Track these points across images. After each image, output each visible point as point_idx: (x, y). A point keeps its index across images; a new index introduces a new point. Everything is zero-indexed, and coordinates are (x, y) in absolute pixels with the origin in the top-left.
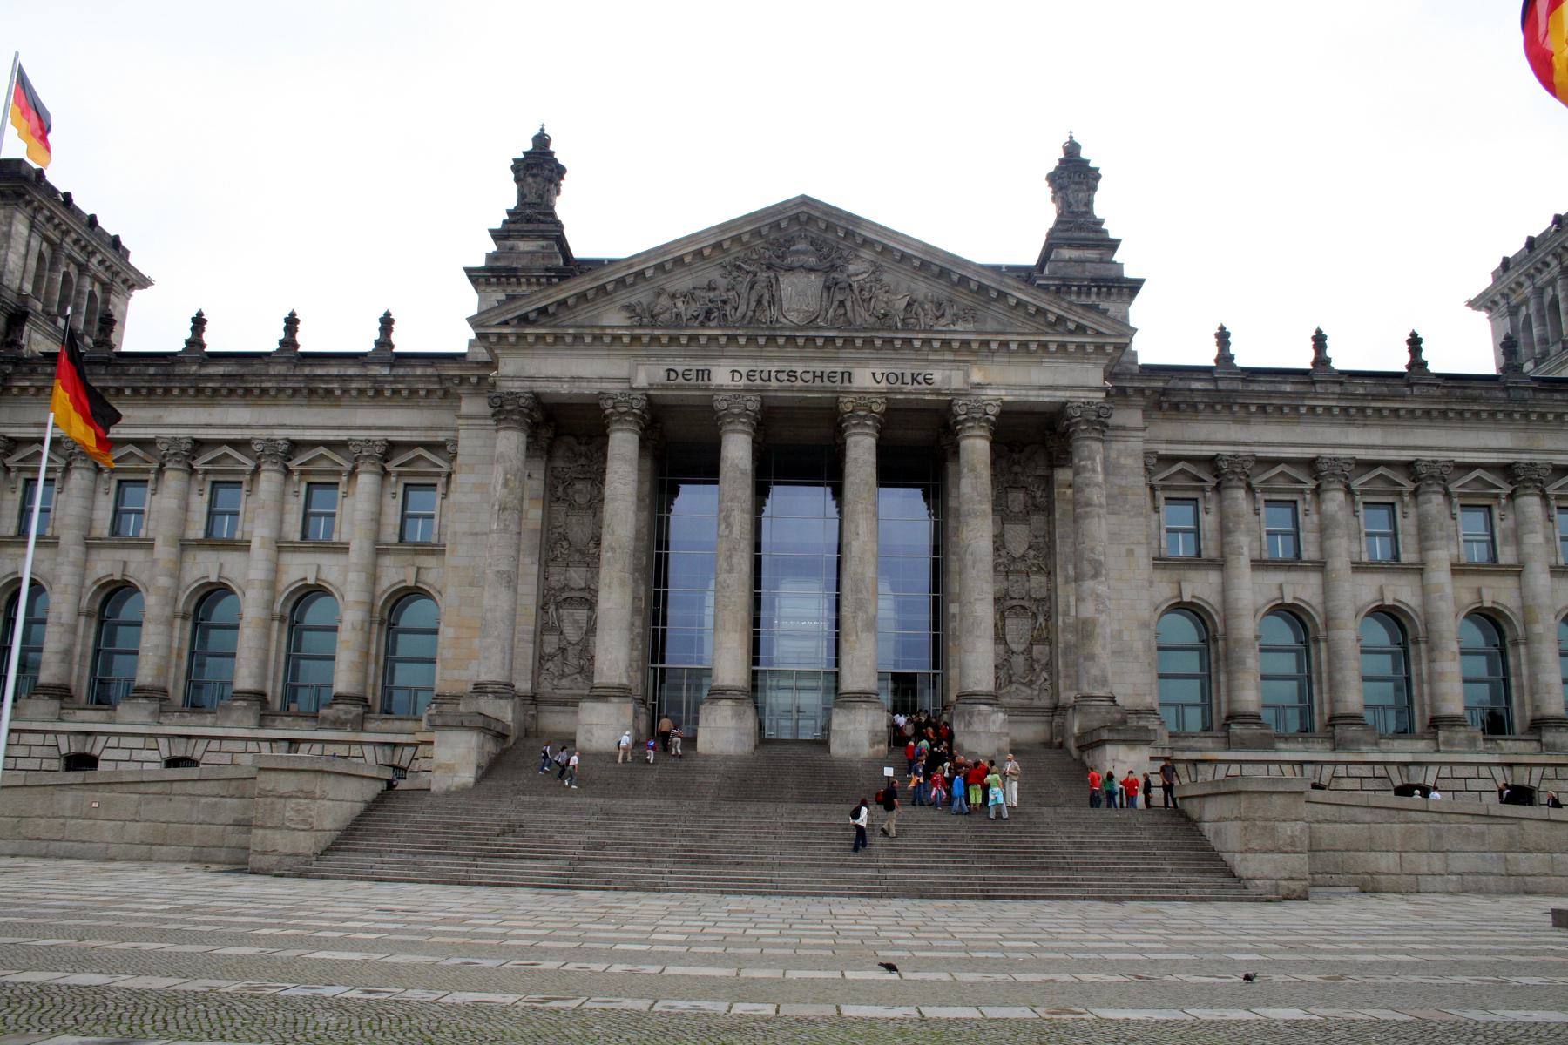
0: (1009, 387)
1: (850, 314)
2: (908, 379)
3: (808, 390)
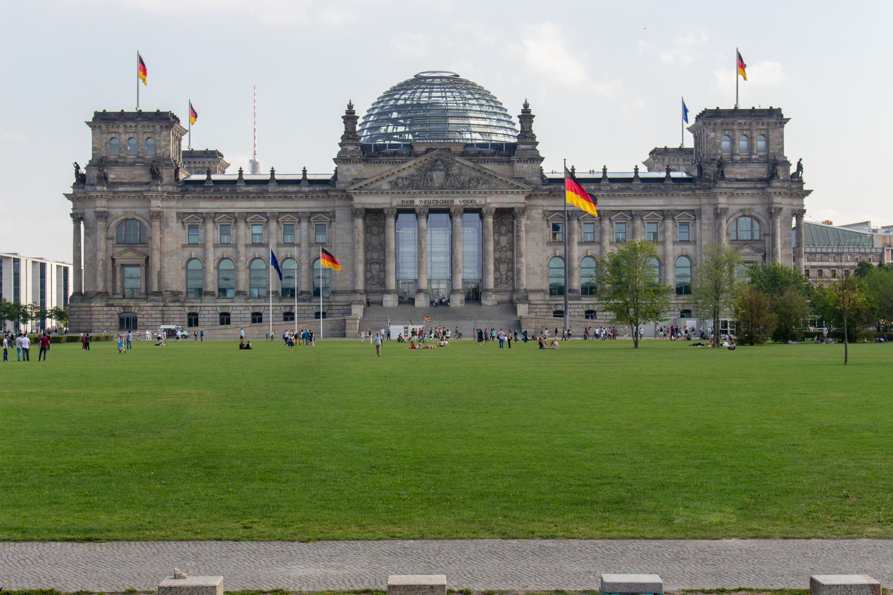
0: (497, 203)
2: (469, 202)
3: (441, 206)
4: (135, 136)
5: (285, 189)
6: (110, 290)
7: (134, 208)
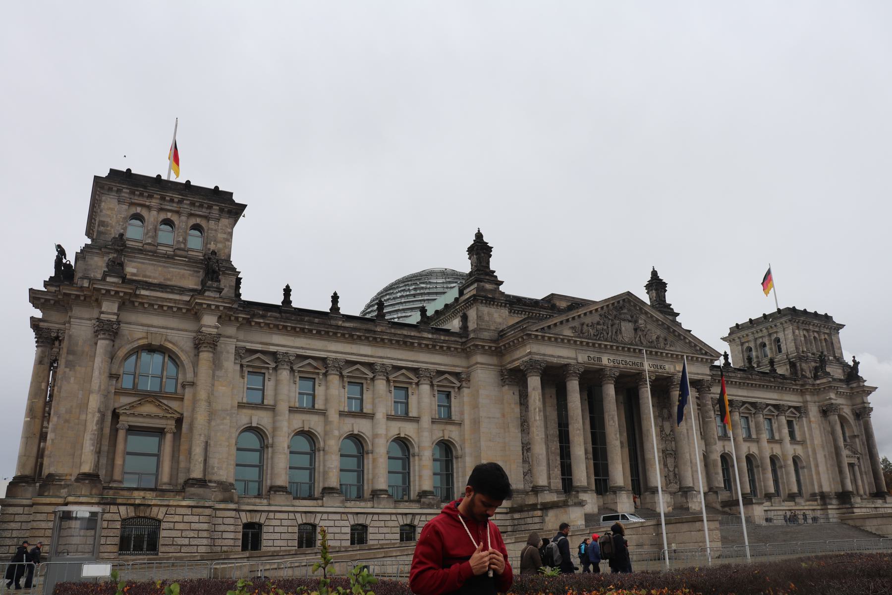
1: (642, 341)
2: (659, 367)
4: (175, 218)
5: (399, 332)
6: (102, 473)
7: (167, 328)
